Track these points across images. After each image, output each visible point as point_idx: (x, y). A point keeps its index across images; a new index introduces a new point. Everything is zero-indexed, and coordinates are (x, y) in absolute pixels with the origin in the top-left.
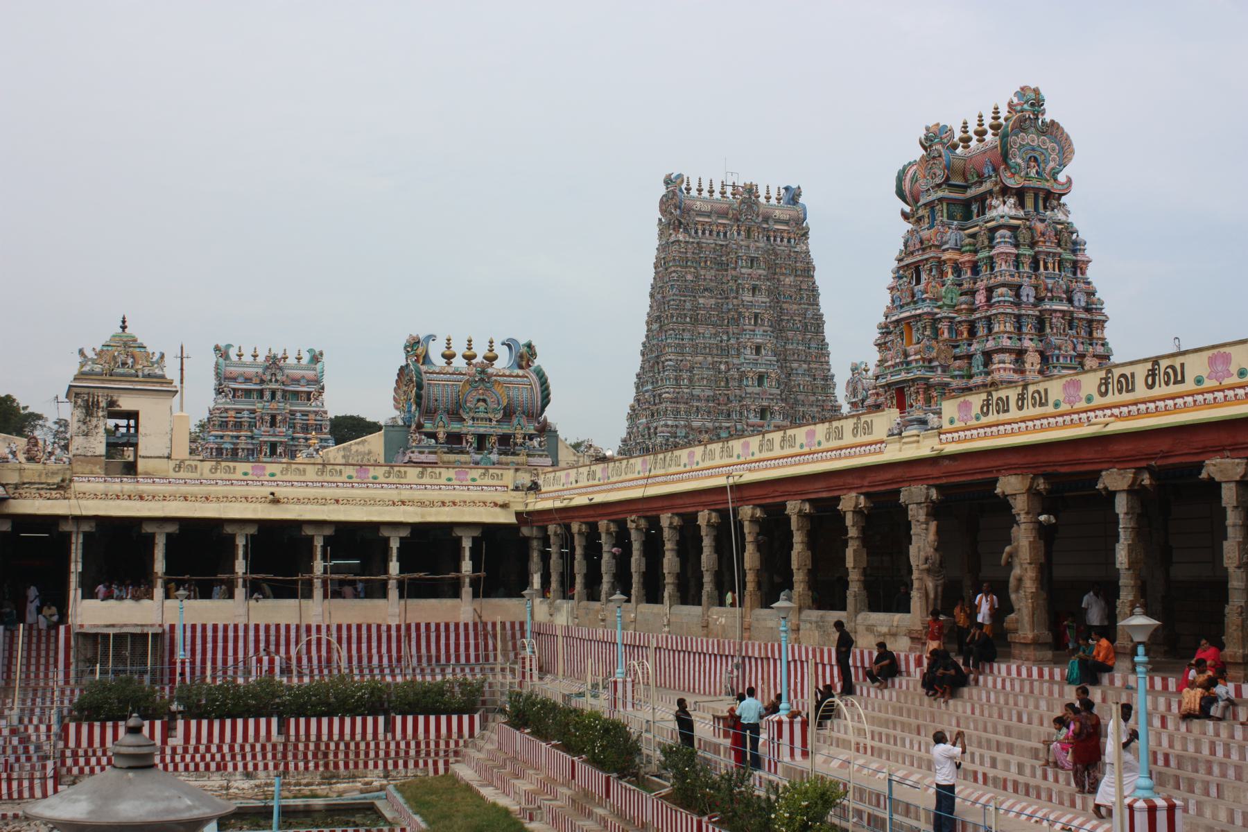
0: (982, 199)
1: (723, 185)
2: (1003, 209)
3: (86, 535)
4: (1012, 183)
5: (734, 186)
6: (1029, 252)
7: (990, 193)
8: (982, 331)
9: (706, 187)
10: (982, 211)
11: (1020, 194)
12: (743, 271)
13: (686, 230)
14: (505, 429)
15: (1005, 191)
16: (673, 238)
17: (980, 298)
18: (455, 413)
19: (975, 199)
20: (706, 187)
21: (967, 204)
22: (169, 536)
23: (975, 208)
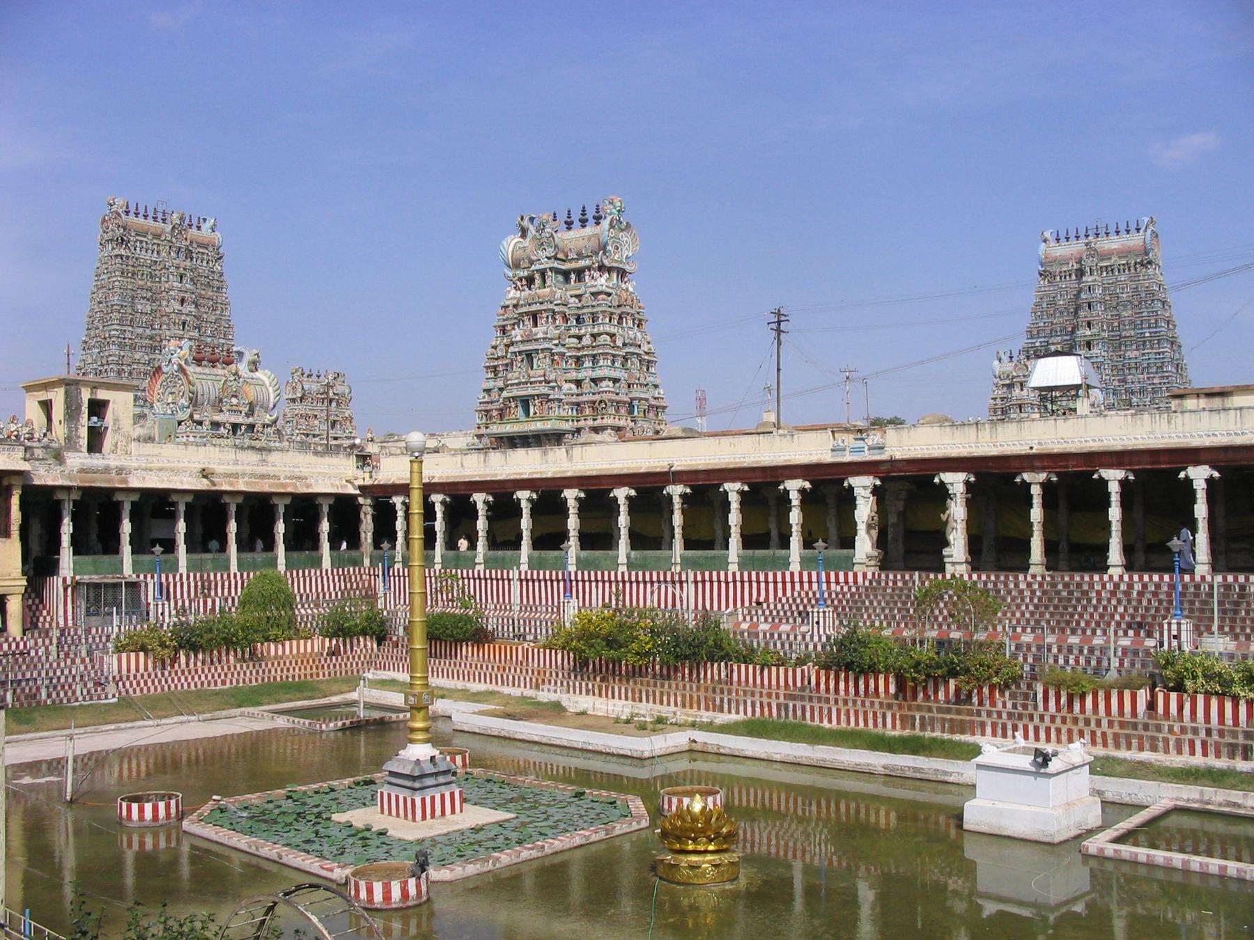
0: (580, 273)
1: (155, 211)
2: (602, 282)
3: (74, 502)
4: (606, 262)
5: (164, 213)
6: (618, 311)
7: (589, 268)
8: (588, 364)
9: (142, 212)
10: (580, 278)
11: (610, 270)
12: (175, 284)
13: (127, 247)
14: (251, 420)
15: (602, 268)
16: (117, 252)
17: (587, 341)
18: (218, 404)
19: (574, 271)
20: (142, 212)
21: (566, 274)
22: (133, 503)
23: (573, 276)
